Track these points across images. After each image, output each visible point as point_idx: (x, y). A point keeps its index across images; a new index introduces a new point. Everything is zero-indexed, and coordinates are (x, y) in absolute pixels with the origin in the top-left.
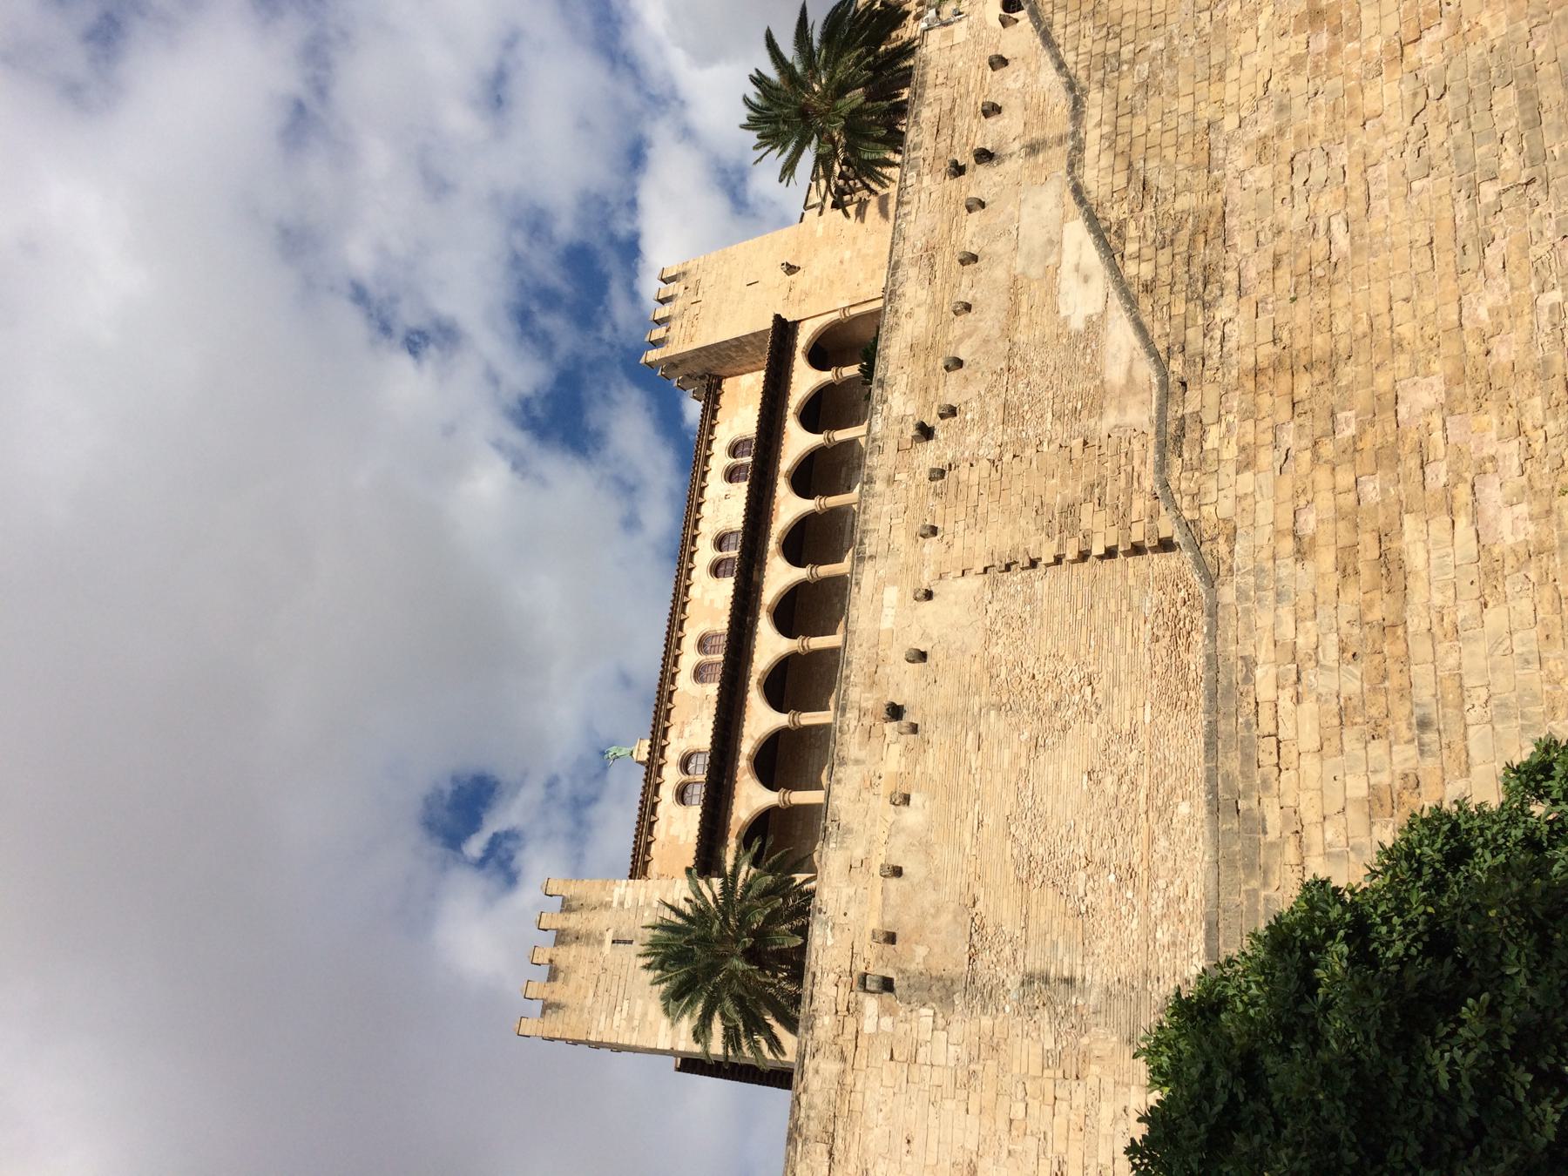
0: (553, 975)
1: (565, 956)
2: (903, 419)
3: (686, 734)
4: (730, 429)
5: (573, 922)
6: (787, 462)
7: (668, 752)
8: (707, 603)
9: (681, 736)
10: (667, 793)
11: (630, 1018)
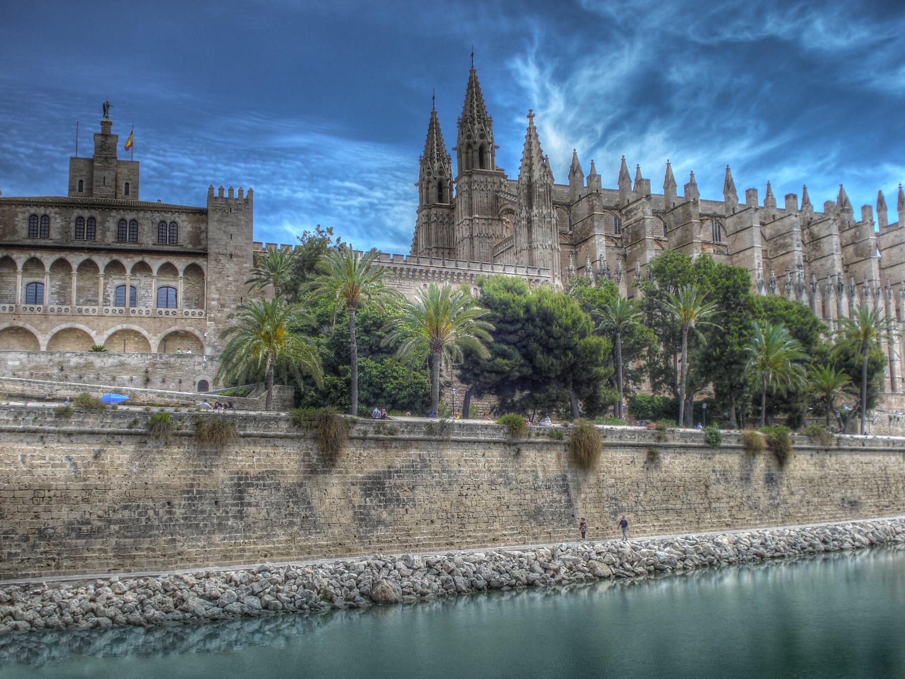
2: (69, 361)
3: (57, 216)
4: (183, 221)
6: (147, 259)
7: (50, 208)
8: (109, 219)
9: (56, 213)
10: (33, 210)
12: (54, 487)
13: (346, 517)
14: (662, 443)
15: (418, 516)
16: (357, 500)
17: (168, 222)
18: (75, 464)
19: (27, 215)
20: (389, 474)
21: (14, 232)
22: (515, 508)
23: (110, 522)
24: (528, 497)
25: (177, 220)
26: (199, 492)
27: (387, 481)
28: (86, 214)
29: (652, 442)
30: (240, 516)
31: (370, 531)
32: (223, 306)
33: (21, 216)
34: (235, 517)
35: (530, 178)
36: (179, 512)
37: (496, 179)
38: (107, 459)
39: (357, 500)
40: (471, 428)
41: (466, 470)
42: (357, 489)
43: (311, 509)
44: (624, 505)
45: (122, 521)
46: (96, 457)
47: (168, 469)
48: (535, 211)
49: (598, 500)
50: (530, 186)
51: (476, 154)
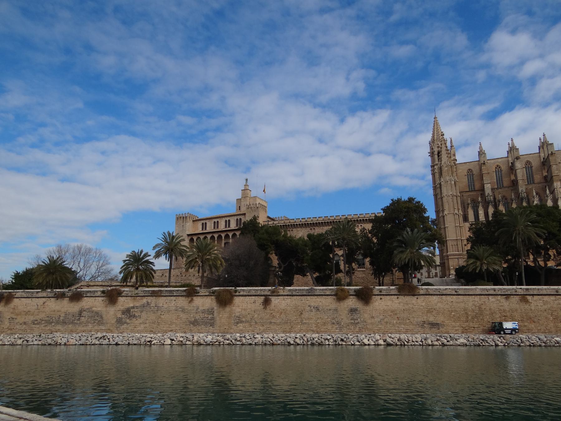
13: (114, 321)
14: (275, 294)
15: (141, 321)
16: (119, 315)
20: (133, 307)
23: (43, 320)
24: (192, 316)
27: (132, 310)
28: (216, 220)
29: (269, 293)
30: (79, 319)
36: (61, 318)
38: (46, 304)
39: (119, 315)
40: (171, 291)
41: (165, 306)
42: (120, 312)
44: (244, 320)
48: (442, 180)
49: (229, 317)
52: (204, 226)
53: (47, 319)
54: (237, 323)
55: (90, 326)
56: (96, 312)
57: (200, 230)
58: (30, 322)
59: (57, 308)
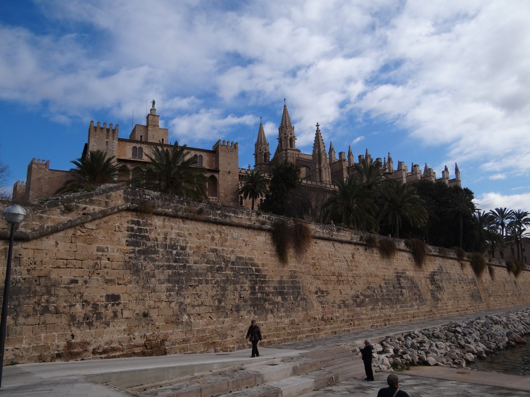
0: (102, 129)
1: (105, 132)
5: (111, 132)
10: (135, 145)
11: (94, 146)
12: (343, 275)
17: (198, 155)
18: (347, 260)
19: (132, 147)
21: (125, 155)
22: (467, 293)
23: (365, 296)
25: (202, 155)
26: (388, 280)
30: (402, 295)
31: (437, 304)
32: (226, 196)
33: (128, 146)
34: (400, 294)
35: (319, 151)
36: (385, 291)
37: (297, 152)
39: (431, 287)
42: (428, 280)
43: (419, 290)
45: (368, 296)
46: (353, 257)
47: (376, 266)
50: (320, 155)
51: (289, 141)
52: (137, 151)
53: (369, 292)
54: (489, 296)
55: (416, 307)
56: (411, 280)
57: (129, 155)
58: (351, 302)
59: (372, 268)
